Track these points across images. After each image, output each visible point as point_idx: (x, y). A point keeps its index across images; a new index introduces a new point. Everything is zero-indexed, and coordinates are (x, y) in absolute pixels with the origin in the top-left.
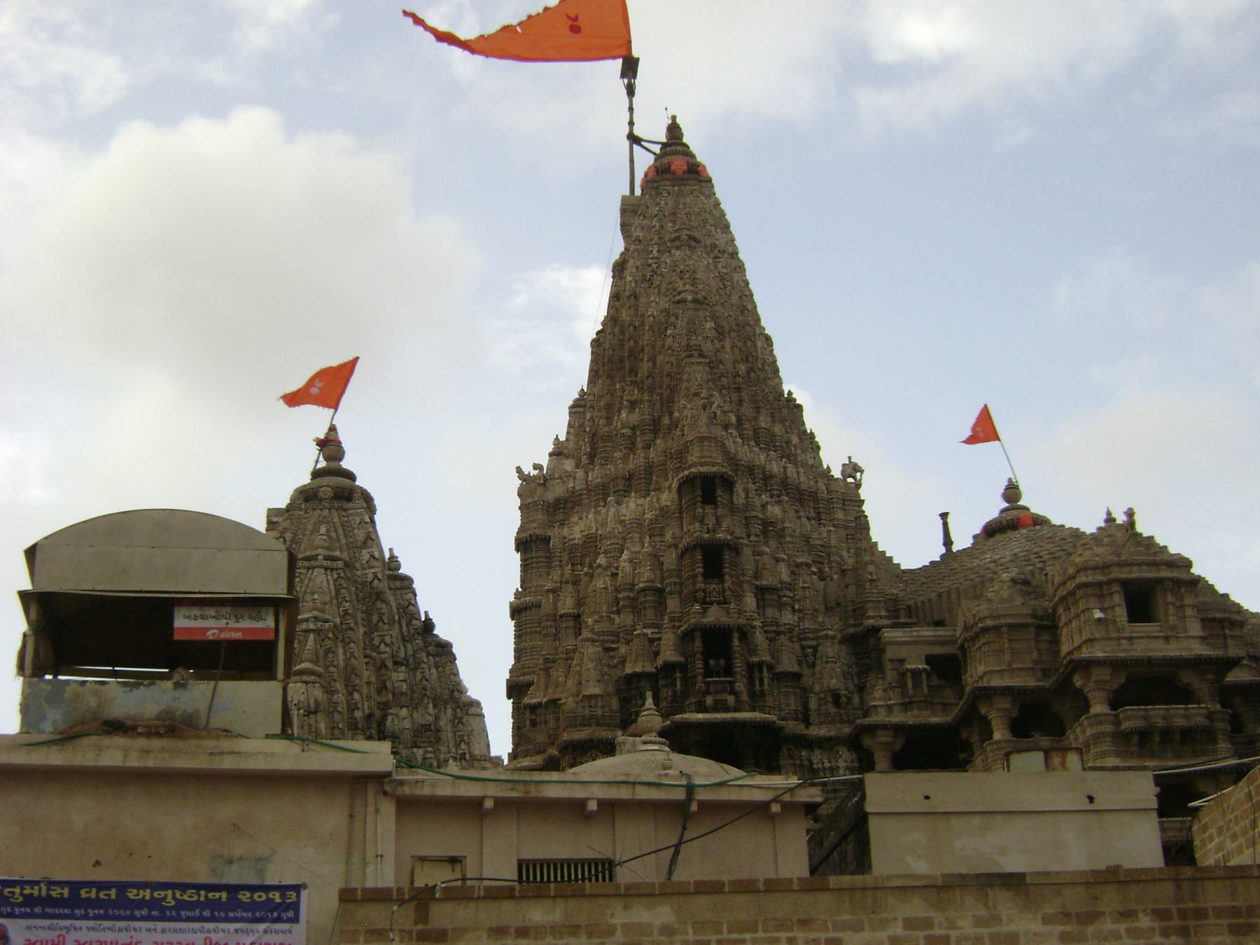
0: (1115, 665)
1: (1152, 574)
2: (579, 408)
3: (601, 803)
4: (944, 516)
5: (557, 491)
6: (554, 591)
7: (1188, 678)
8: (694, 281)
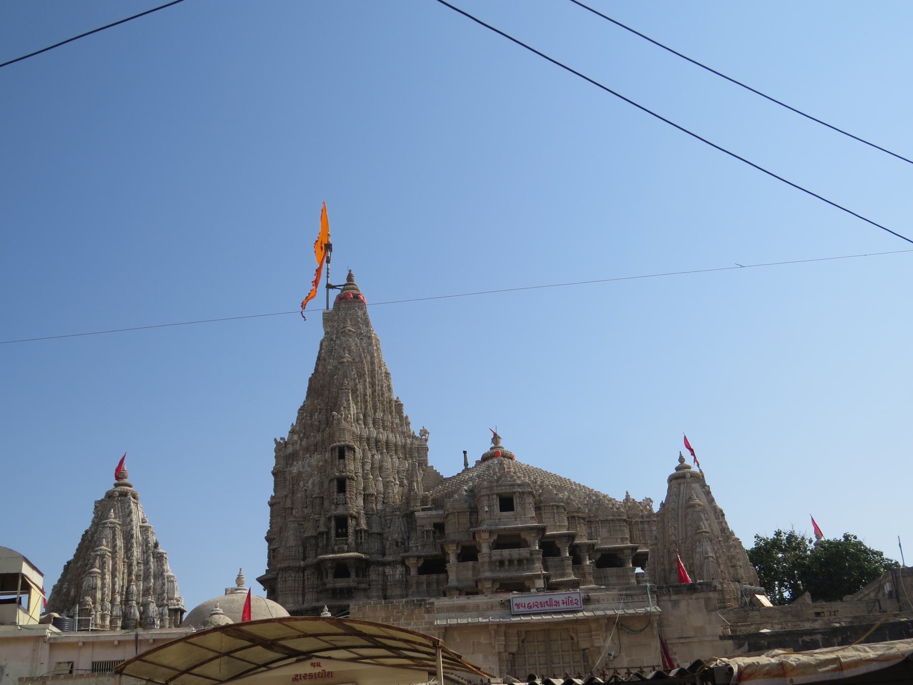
0: (491, 532)
1: (509, 491)
2: (302, 410)
3: (119, 642)
4: (465, 452)
5: (290, 450)
6: (286, 496)
7: (523, 535)
8: (350, 352)
